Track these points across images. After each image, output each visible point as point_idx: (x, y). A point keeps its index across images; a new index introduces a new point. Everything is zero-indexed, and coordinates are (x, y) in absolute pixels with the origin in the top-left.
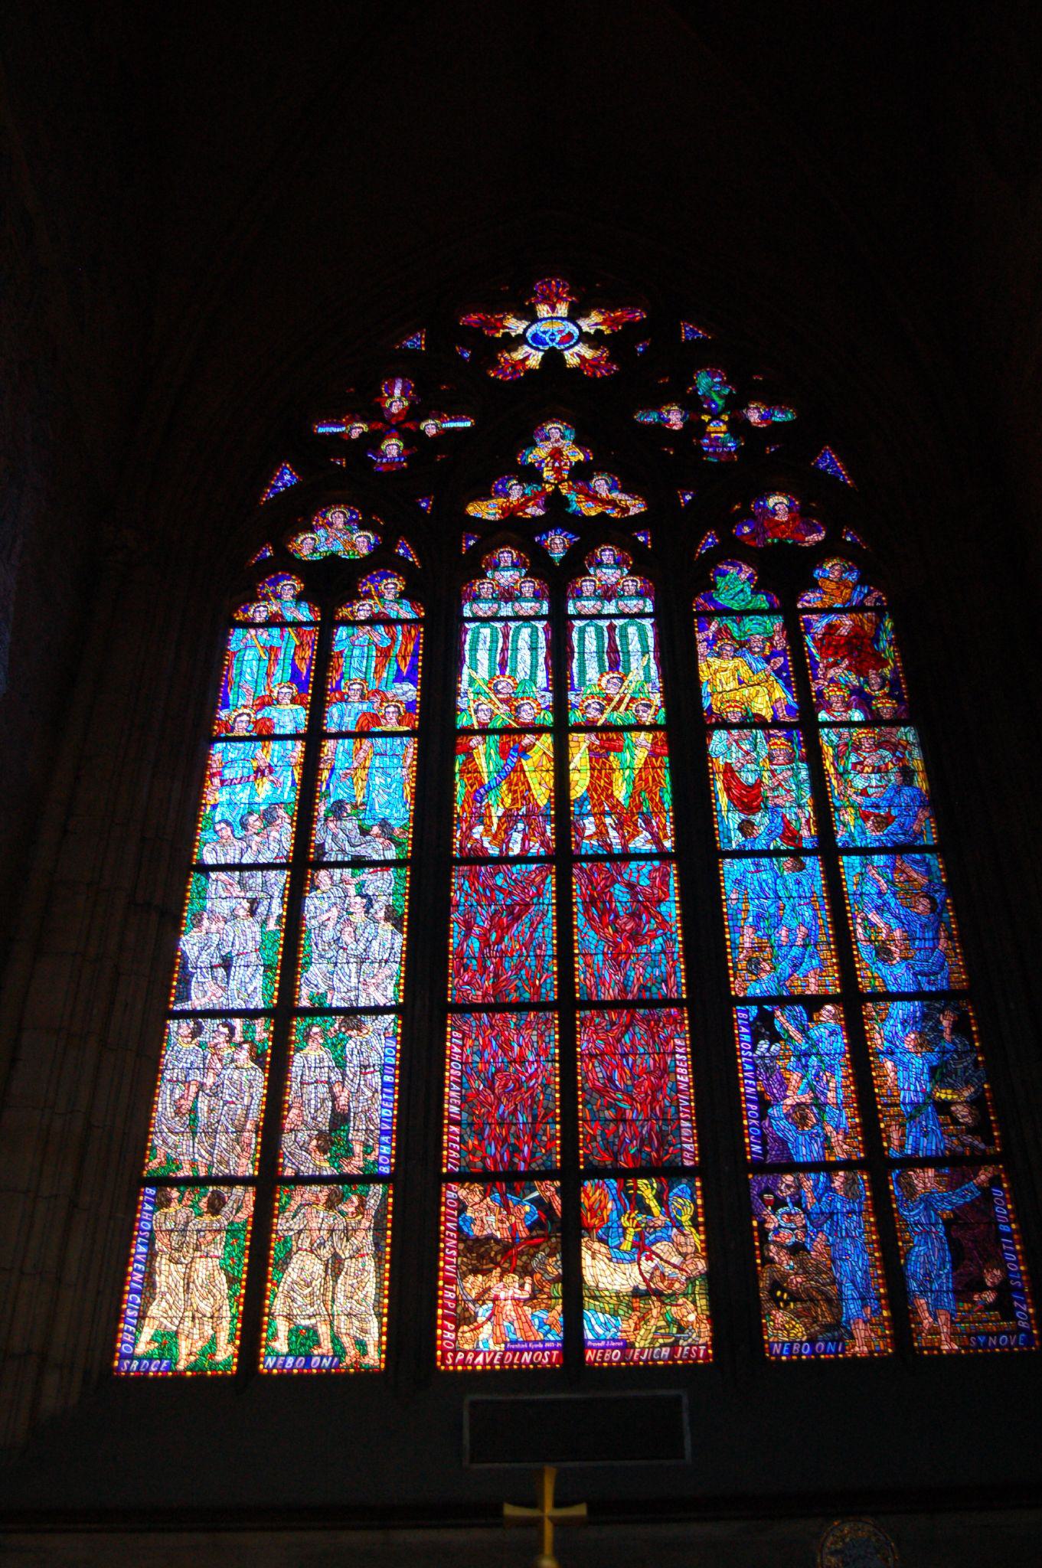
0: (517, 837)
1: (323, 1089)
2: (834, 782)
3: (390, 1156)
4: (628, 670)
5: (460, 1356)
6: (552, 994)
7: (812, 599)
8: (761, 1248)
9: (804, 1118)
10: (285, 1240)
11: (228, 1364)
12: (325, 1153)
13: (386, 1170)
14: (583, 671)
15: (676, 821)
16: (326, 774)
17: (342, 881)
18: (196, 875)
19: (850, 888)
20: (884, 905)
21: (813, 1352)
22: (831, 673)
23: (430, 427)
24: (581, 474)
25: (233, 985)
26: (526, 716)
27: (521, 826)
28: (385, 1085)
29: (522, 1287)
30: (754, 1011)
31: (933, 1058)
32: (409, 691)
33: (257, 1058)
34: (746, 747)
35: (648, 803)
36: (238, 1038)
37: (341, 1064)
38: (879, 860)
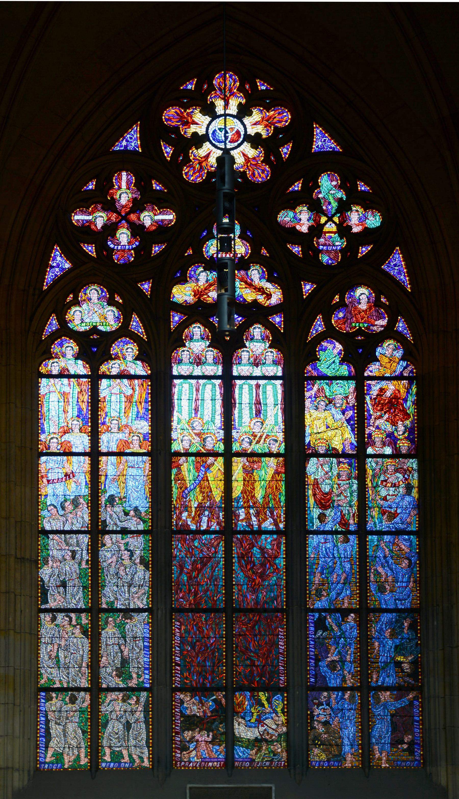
0: (205, 519)
1: (116, 648)
2: (370, 492)
3: (149, 680)
5: (183, 763)
6: (222, 605)
7: (374, 369)
8: (311, 722)
11: (85, 765)
12: (120, 678)
13: (148, 686)
14: (240, 417)
16: (103, 478)
17: (117, 542)
18: (42, 536)
19: (370, 553)
21: (329, 765)
22: (378, 422)
23: (147, 219)
25: (69, 596)
26: (209, 446)
27: (207, 513)
29: (208, 736)
30: (317, 615)
33: (84, 632)
34: (327, 468)
35: (273, 502)
36: (74, 622)
38: (387, 538)
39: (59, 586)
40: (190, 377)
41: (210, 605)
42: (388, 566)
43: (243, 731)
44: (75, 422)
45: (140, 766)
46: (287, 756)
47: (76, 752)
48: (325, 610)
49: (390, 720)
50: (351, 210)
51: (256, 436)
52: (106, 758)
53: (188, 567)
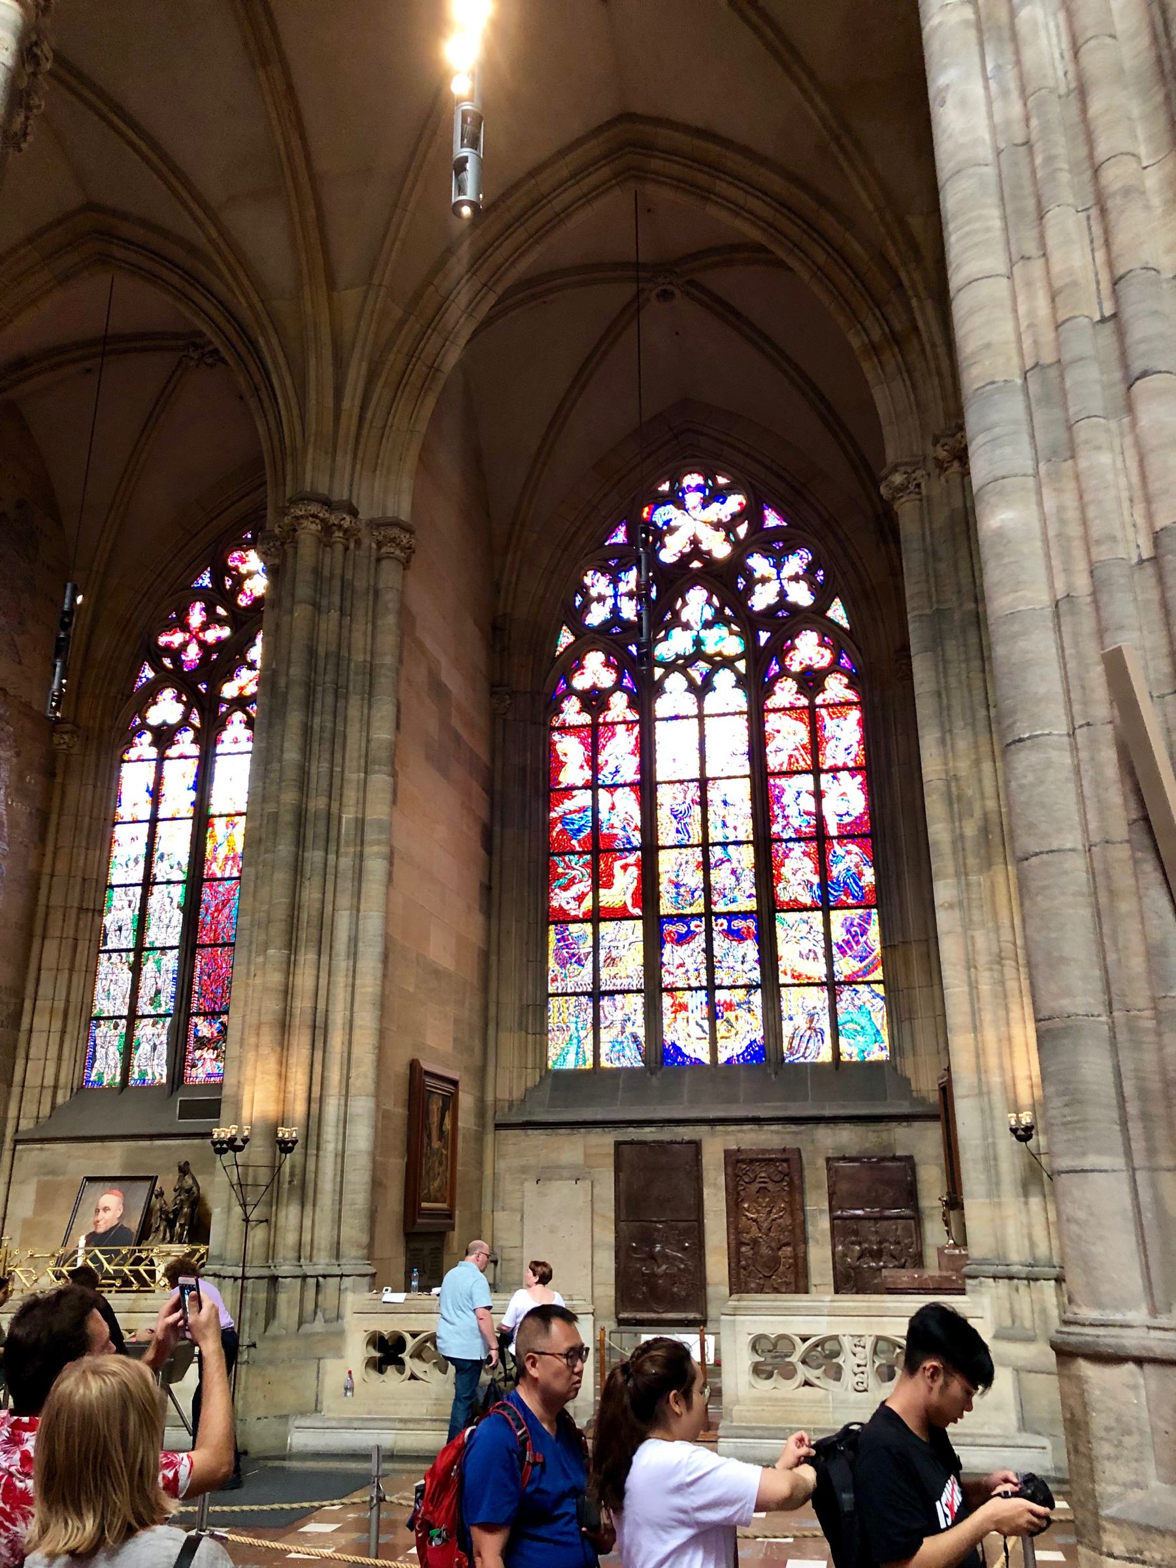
27: (230, 862)
33: (130, 969)
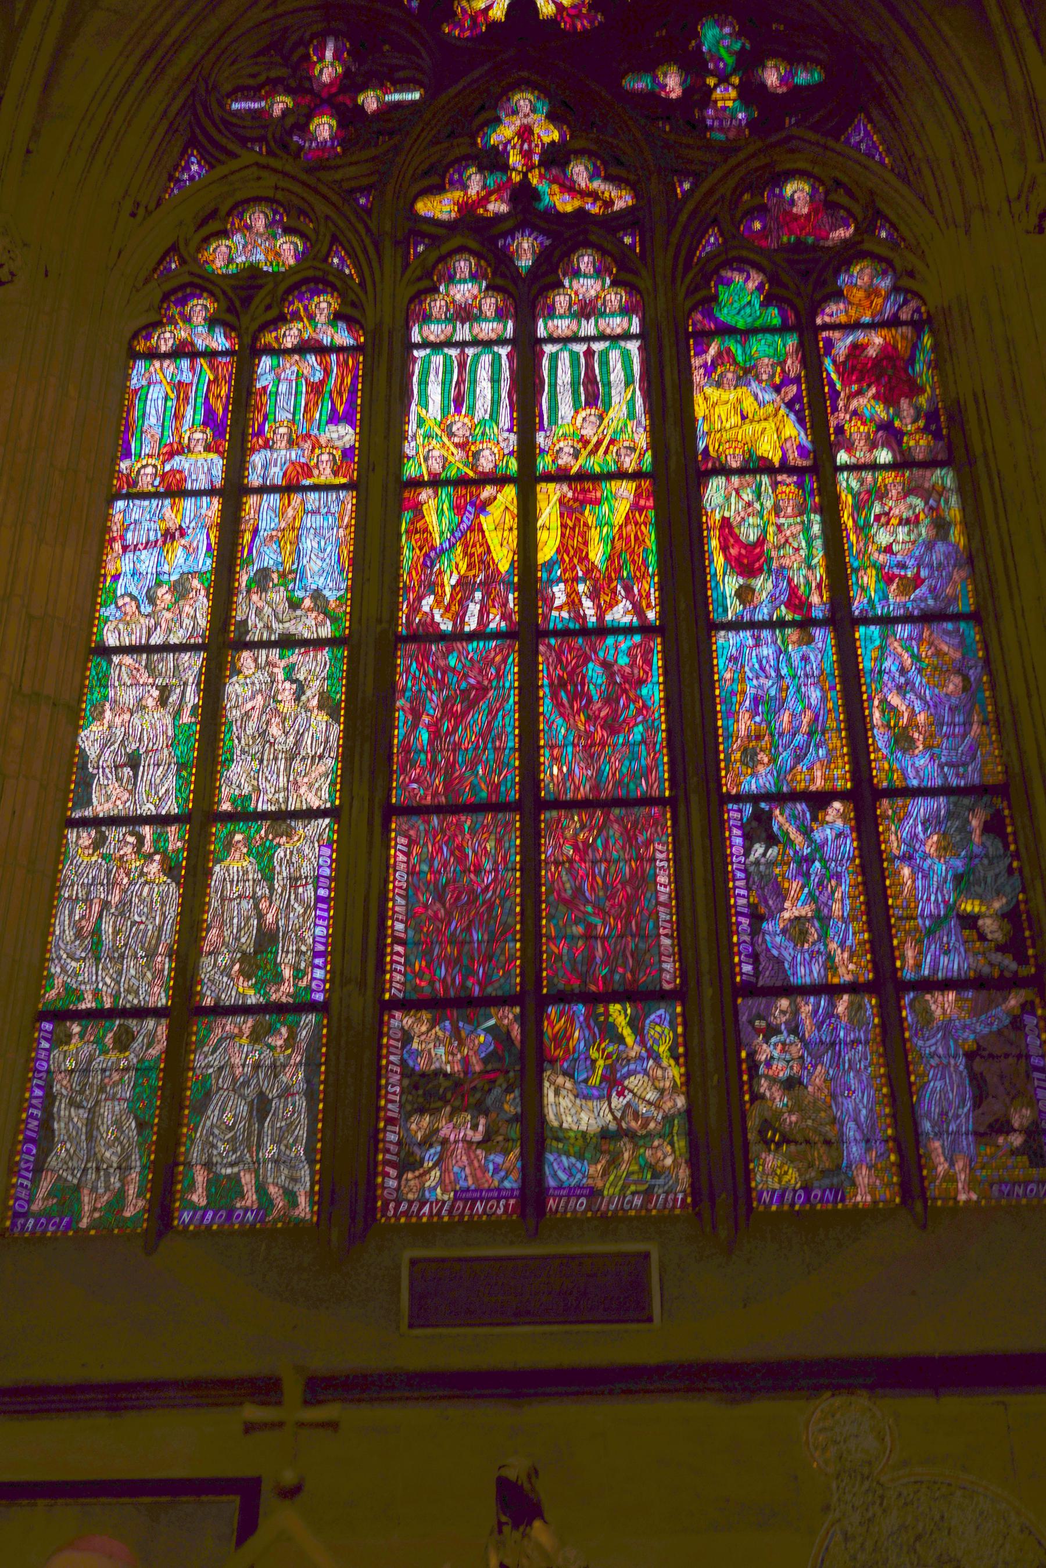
0: (474, 609)
1: (246, 905)
2: (853, 538)
3: (324, 981)
4: (608, 405)
5: (404, 1207)
7: (834, 312)
9: (804, 934)
10: (206, 1078)
11: (135, 1219)
12: (249, 978)
13: (319, 997)
14: (554, 408)
15: (661, 588)
16: (247, 536)
17: (268, 663)
20: (907, 684)
21: (808, 1199)
22: (854, 404)
23: (370, 101)
24: (555, 159)
25: (142, 787)
26: (486, 464)
27: (478, 595)
28: (319, 899)
29: (475, 1127)
30: (748, 809)
31: (958, 863)
32: (345, 435)
33: (170, 870)
34: (748, 495)
36: (147, 847)
37: (268, 876)
38: (903, 631)
39: (122, 766)
40: (449, 343)
41: (484, 794)
42: (913, 689)
43: (568, 1110)
44: (198, 435)
45: (285, 1217)
46: (692, 1175)
47: (115, 1181)
48: (767, 797)
49: (966, 1067)
50: (764, 67)
51: (588, 442)
52: (195, 1198)
53: (431, 712)
